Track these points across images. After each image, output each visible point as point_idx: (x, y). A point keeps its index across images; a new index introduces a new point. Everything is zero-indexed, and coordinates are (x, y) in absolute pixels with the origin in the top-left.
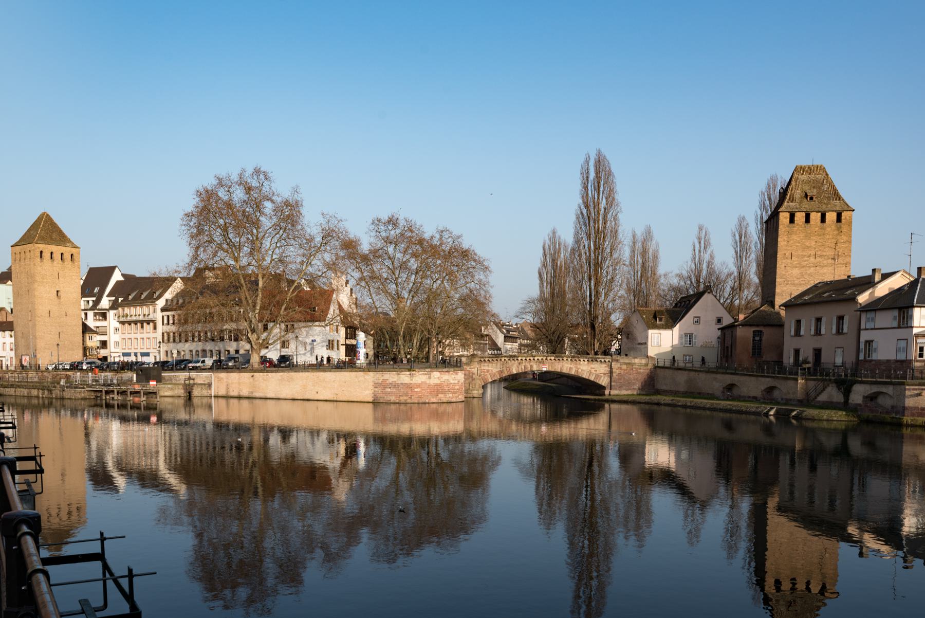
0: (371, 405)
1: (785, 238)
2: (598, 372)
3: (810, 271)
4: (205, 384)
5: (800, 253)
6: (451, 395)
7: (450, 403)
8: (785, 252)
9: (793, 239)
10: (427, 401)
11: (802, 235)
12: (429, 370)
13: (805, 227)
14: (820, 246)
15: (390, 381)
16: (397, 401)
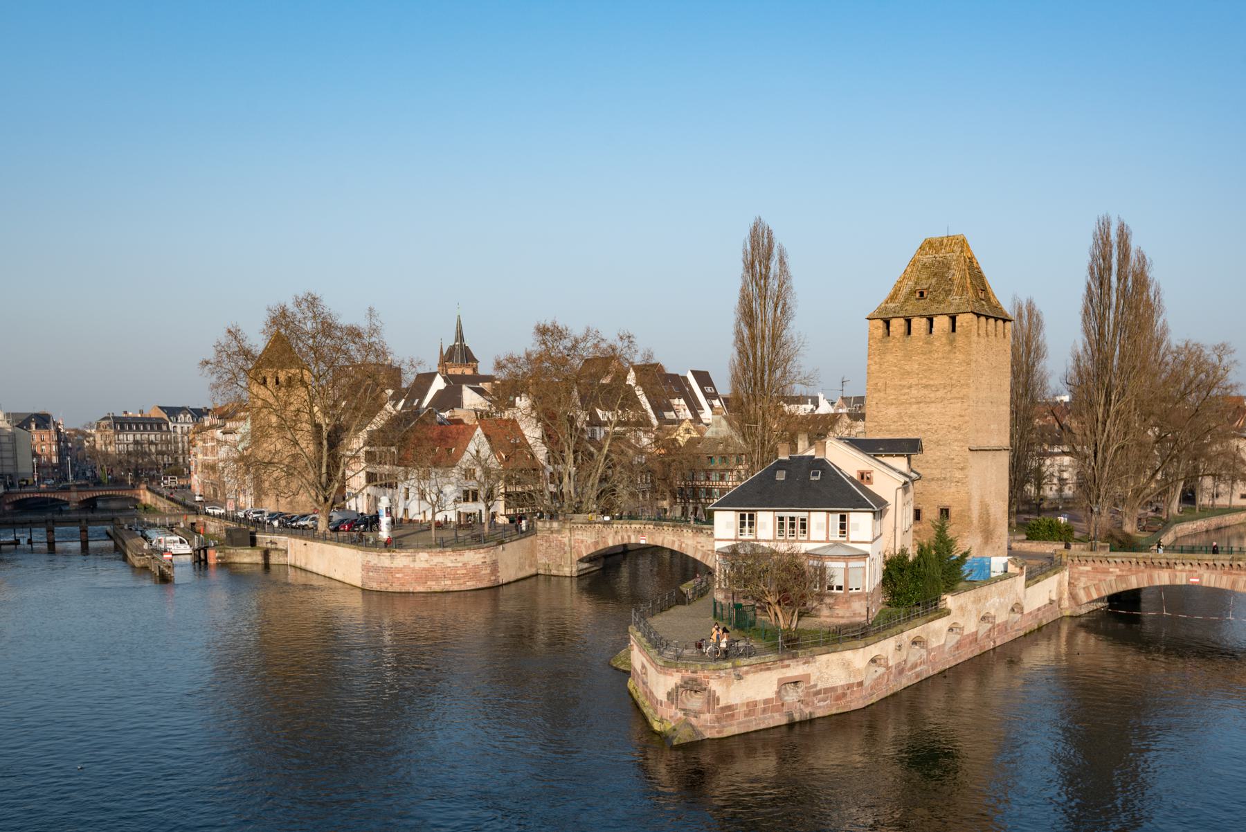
0: (359, 592)
1: (877, 359)
2: (705, 548)
3: (912, 410)
4: (281, 550)
5: (897, 382)
6: (449, 582)
7: (448, 592)
8: (877, 380)
9: (888, 361)
10: (411, 590)
11: (900, 354)
12: (412, 550)
13: (904, 341)
14: (925, 370)
15: (371, 564)
16: (379, 589)
